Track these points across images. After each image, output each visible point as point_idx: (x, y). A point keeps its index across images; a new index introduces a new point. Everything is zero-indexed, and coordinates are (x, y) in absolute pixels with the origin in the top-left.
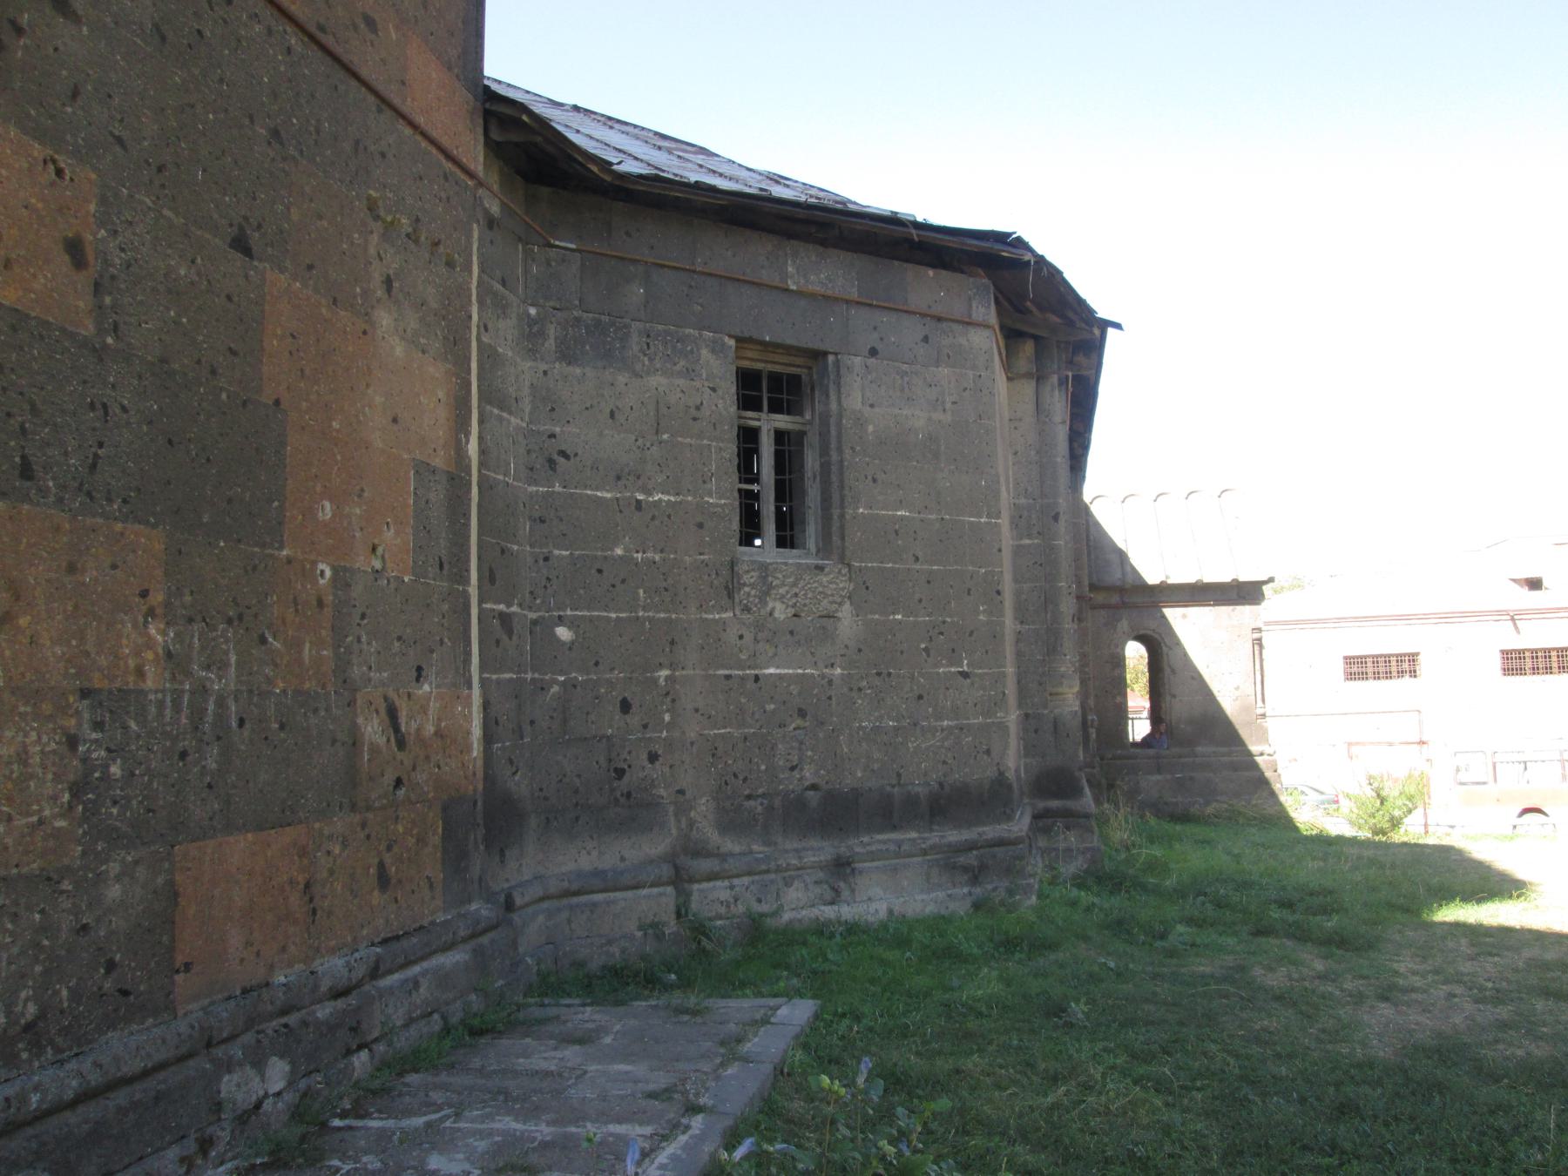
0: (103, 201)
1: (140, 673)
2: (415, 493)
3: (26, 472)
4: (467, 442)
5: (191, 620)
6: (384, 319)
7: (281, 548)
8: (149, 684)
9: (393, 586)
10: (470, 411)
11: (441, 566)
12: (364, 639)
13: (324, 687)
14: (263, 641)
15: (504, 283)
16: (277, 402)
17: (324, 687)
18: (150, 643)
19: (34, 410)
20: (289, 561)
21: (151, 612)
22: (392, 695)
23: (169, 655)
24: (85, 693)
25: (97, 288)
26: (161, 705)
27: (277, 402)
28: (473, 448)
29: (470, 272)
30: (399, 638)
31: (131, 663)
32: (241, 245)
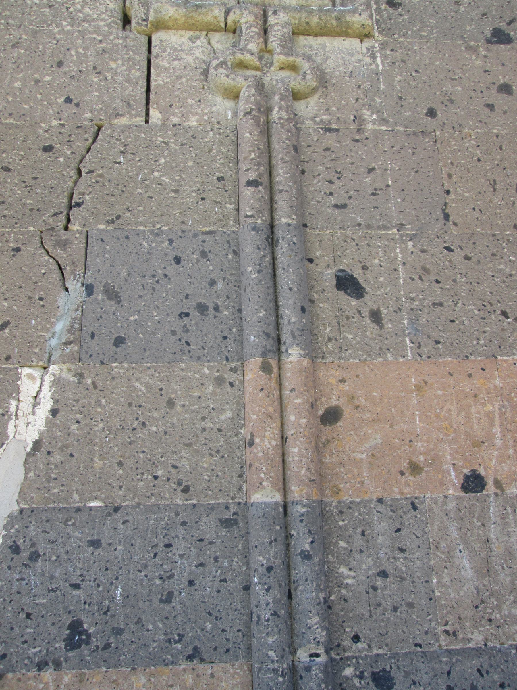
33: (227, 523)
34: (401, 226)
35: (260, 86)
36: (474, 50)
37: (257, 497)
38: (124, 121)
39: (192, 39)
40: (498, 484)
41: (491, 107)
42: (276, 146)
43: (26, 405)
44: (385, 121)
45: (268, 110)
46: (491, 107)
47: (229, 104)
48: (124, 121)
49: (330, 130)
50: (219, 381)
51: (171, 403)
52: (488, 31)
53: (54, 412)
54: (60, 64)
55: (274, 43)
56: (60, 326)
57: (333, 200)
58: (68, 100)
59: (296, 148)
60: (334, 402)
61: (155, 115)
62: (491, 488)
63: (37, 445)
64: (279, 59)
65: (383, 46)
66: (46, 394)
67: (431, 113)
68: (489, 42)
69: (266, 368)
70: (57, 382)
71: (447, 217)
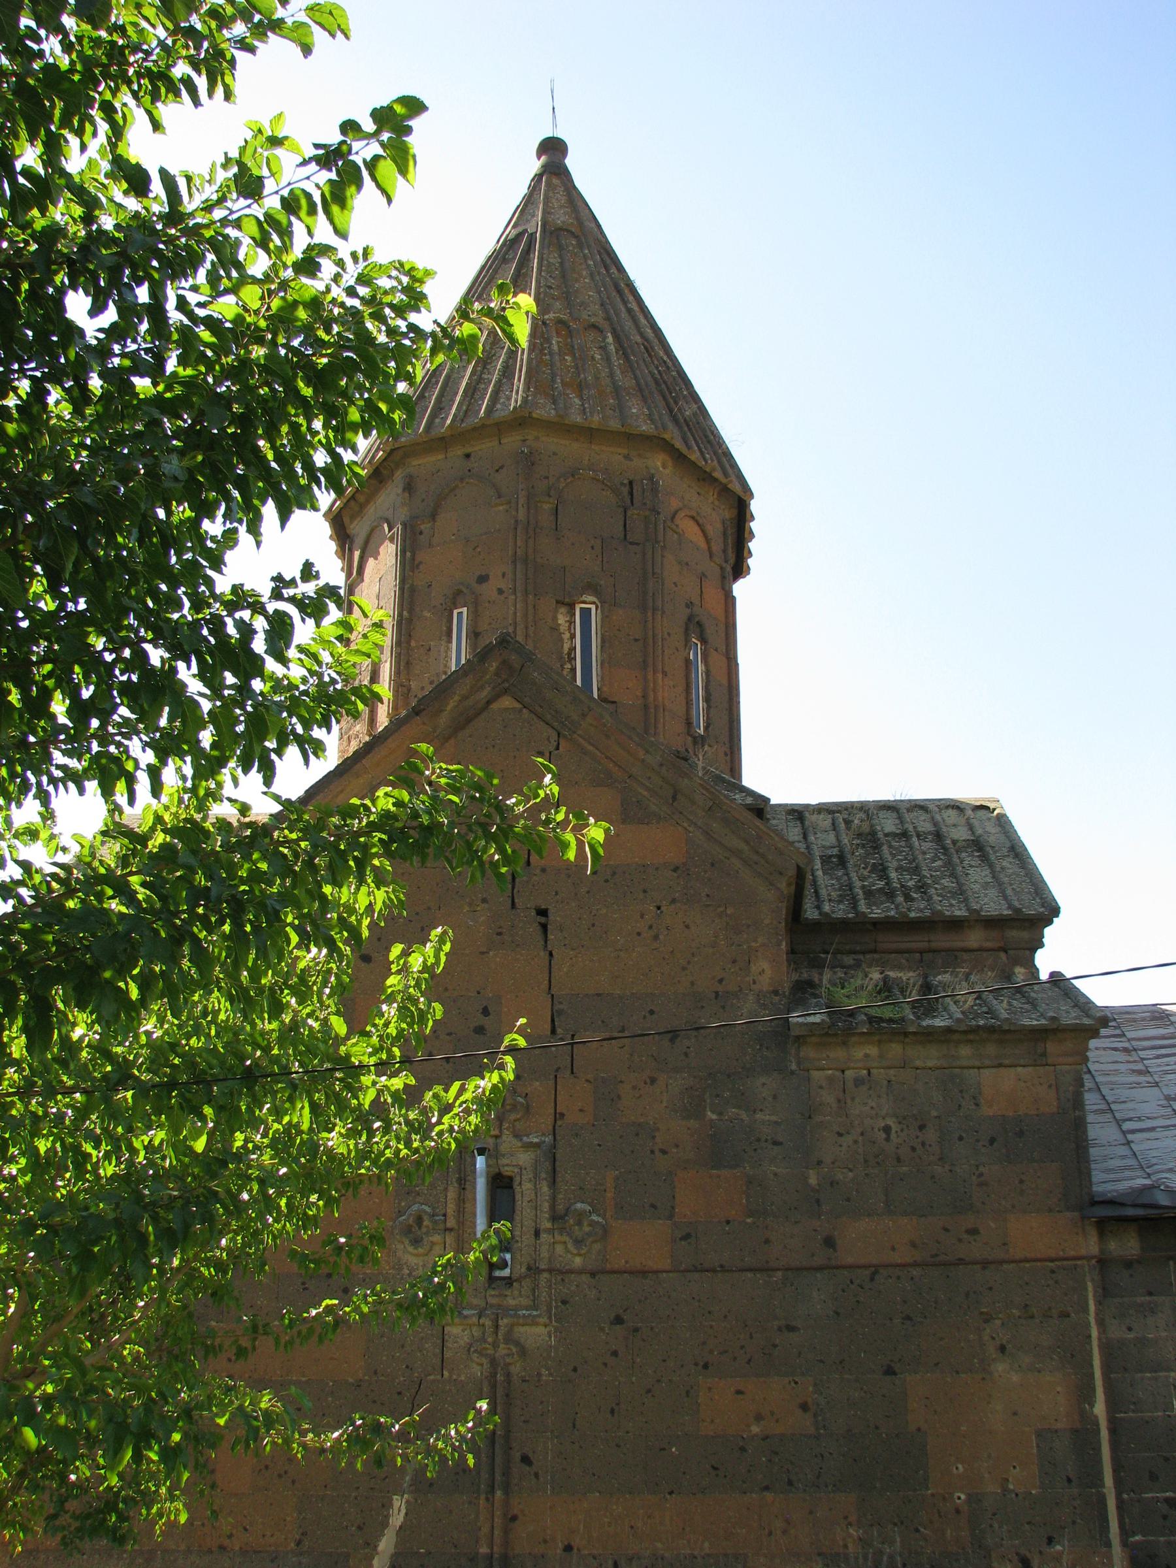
0: (815, 1385)
1: (846, 1546)
2: (1038, 1446)
3: (790, 1483)
4: (1092, 1405)
5: (872, 1525)
6: (1000, 1367)
7: (927, 1488)
8: (851, 1550)
9: (1020, 1497)
10: (1094, 1390)
11: (1069, 1480)
12: (996, 1525)
13: (963, 1549)
14: (917, 1530)
15: (1150, 1294)
16: (919, 1430)
17: (963, 1549)
18: (850, 1536)
19: (792, 1463)
20: (933, 1495)
21: (850, 1524)
22: (1023, 1551)
23: (860, 1539)
24: (819, 1554)
25: (815, 1415)
26: (856, 1558)
27: (919, 1430)
28: (1100, 1409)
29: (1086, 1310)
30: (1029, 1523)
31: (841, 1543)
32: (890, 1371)
33: (471, 1560)
34: (552, 1432)
35: (493, 1362)
36: (602, 1329)
37: (481, 1550)
38: (432, 1377)
39: (463, 1331)
40: (578, 1550)
41: (605, 1364)
42: (498, 1395)
43: (396, 1511)
44: (551, 1374)
45: (496, 1373)
46: (605, 1364)
47: (479, 1368)
48: (432, 1377)
49: (524, 1381)
50: (470, 1503)
51: (451, 1512)
52: (612, 1316)
53: (406, 1514)
54: (403, 1346)
55: (500, 1337)
56: (407, 1478)
57: (523, 1418)
58: (407, 1367)
59: (507, 1395)
60: (515, 1512)
61: (446, 1373)
62: (575, 1550)
63: (401, 1527)
64: (502, 1346)
65: (556, 1329)
66: (403, 1507)
67: (575, 1370)
68: (612, 1323)
69: (487, 1499)
70: (407, 1502)
71: (574, 1426)
